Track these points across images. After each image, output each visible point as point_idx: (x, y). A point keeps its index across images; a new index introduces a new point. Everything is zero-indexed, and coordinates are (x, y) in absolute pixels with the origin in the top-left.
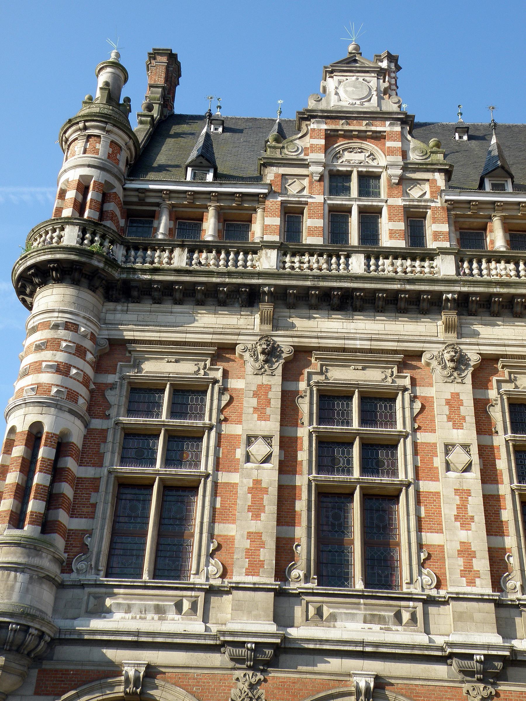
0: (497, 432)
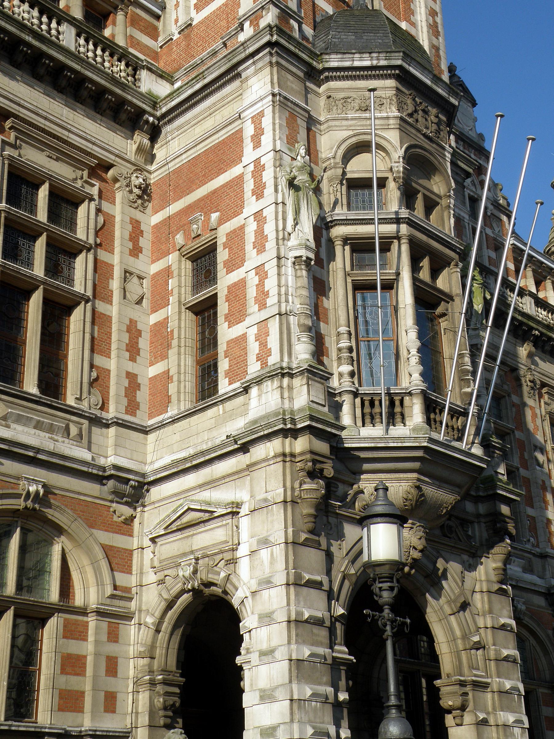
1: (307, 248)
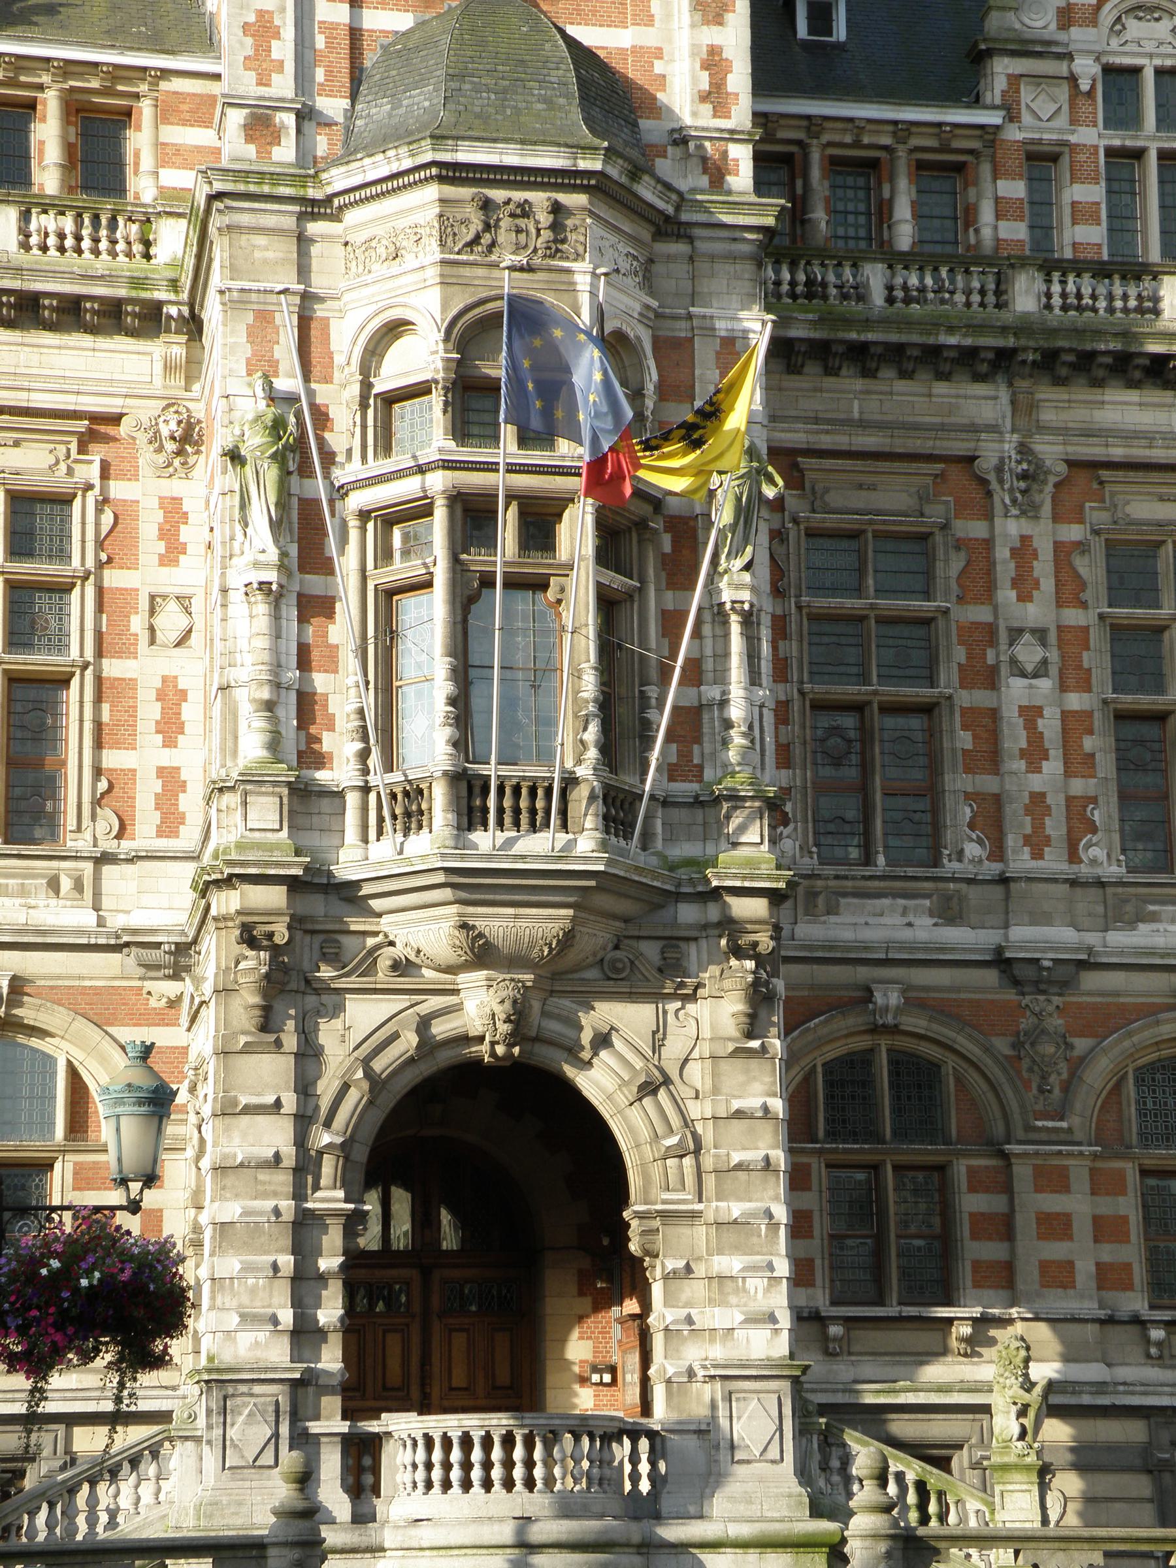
1: (257, 565)
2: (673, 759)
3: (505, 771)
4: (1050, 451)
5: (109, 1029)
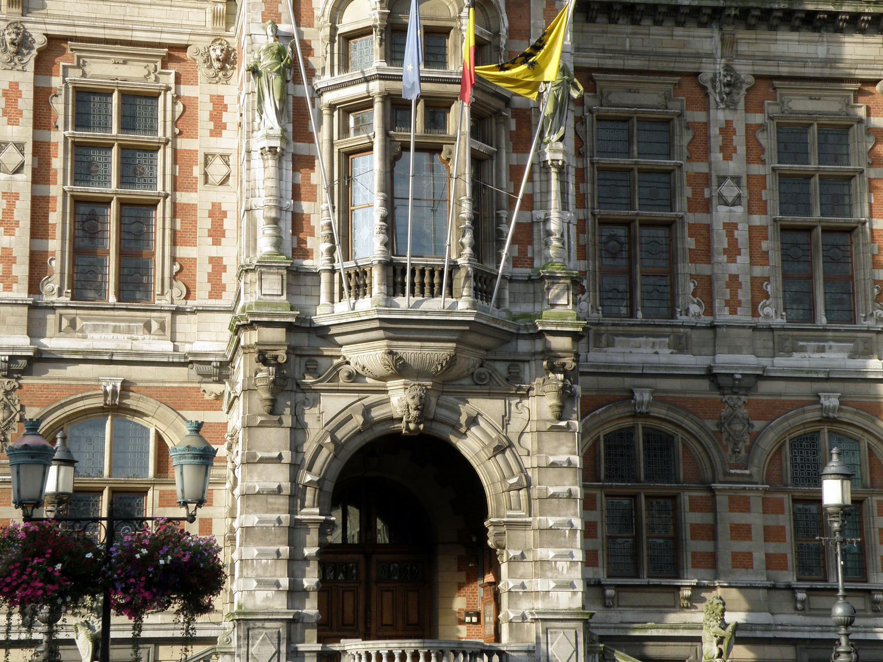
0: (57, 127)
1: (268, 136)
2: (516, 254)
3: (416, 261)
4: (744, 69)
5: (181, 412)
